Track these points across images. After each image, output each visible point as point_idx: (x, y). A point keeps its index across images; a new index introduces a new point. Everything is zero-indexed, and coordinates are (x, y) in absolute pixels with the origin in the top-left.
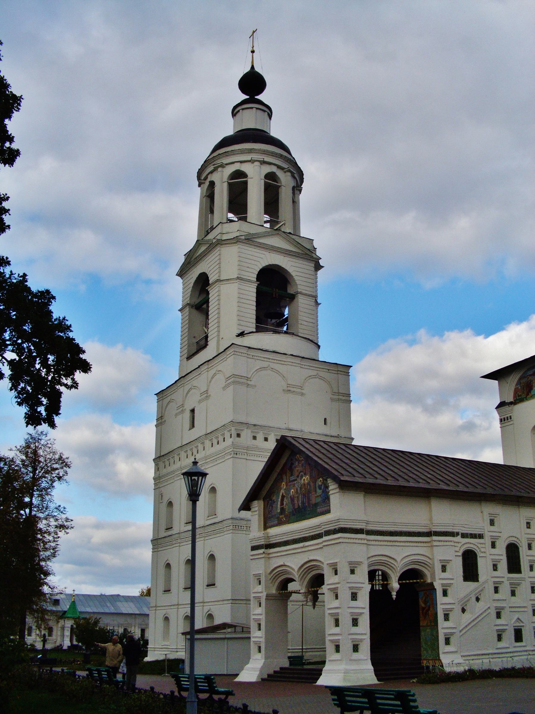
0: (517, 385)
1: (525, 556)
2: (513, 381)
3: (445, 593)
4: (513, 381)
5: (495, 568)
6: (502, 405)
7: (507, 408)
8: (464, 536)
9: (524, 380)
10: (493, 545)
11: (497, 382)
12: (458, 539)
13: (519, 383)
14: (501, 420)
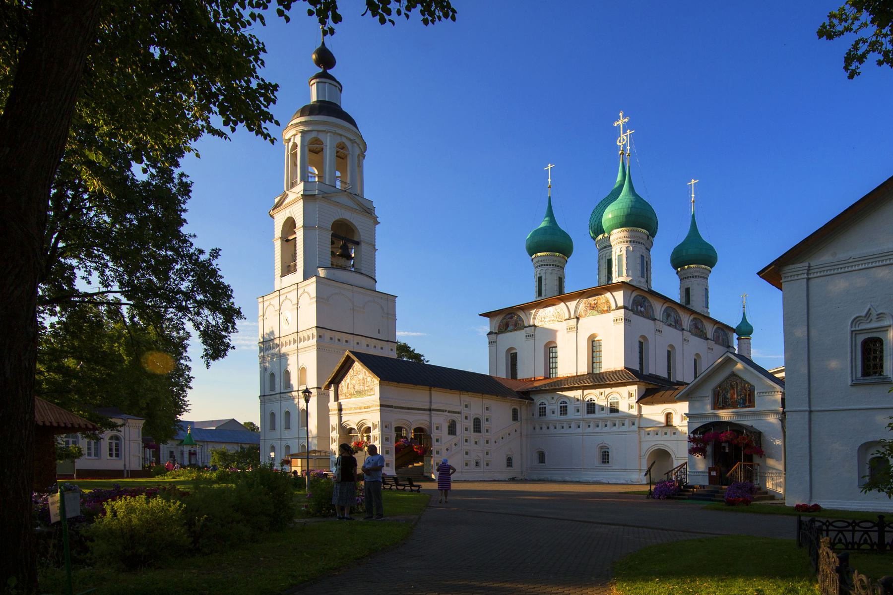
0: (500, 322)
1: (484, 425)
2: (498, 320)
3: (437, 440)
4: (498, 320)
5: (466, 429)
6: (490, 334)
7: (494, 336)
8: (449, 412)
9: (505, 321)
10: (466, 418)
11: (489, 319)
12: (446, 413)
13: (501, 322)
14: (489, 343)
